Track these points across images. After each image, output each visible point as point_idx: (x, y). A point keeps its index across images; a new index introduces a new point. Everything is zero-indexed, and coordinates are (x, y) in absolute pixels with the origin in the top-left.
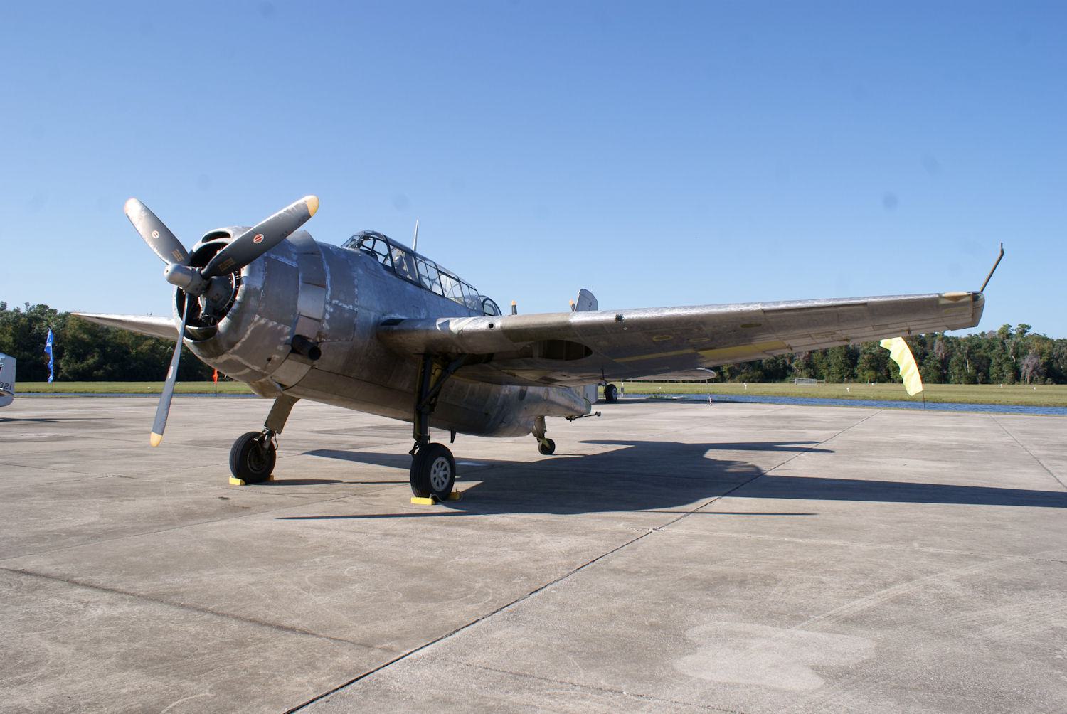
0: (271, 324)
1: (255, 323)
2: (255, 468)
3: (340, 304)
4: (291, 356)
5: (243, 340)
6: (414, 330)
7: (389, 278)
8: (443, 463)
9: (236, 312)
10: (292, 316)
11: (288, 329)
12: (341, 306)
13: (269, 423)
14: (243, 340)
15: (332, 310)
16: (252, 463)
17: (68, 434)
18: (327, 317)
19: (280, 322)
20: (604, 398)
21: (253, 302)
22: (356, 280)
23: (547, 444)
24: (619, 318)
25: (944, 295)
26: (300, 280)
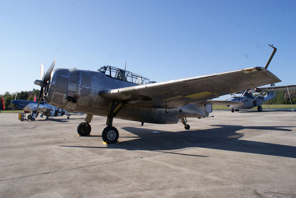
0: (59, 94)
1: (54, 94)
3: (85, 87)
5: (52, 98)
7: (108, 78)
8: (112, 132)
10: (67, 92)
11: (65, 95)
12: (85, 88)
13: (86, 120)
14: (52, 98)
15: (81, 89)
16: (83, 131)
18: (80, 91)
19: (62, 93)
20: (257, 110)
21: (53, 88)
23: (187, 126)
25: (244, 69)
26: (69, 81)
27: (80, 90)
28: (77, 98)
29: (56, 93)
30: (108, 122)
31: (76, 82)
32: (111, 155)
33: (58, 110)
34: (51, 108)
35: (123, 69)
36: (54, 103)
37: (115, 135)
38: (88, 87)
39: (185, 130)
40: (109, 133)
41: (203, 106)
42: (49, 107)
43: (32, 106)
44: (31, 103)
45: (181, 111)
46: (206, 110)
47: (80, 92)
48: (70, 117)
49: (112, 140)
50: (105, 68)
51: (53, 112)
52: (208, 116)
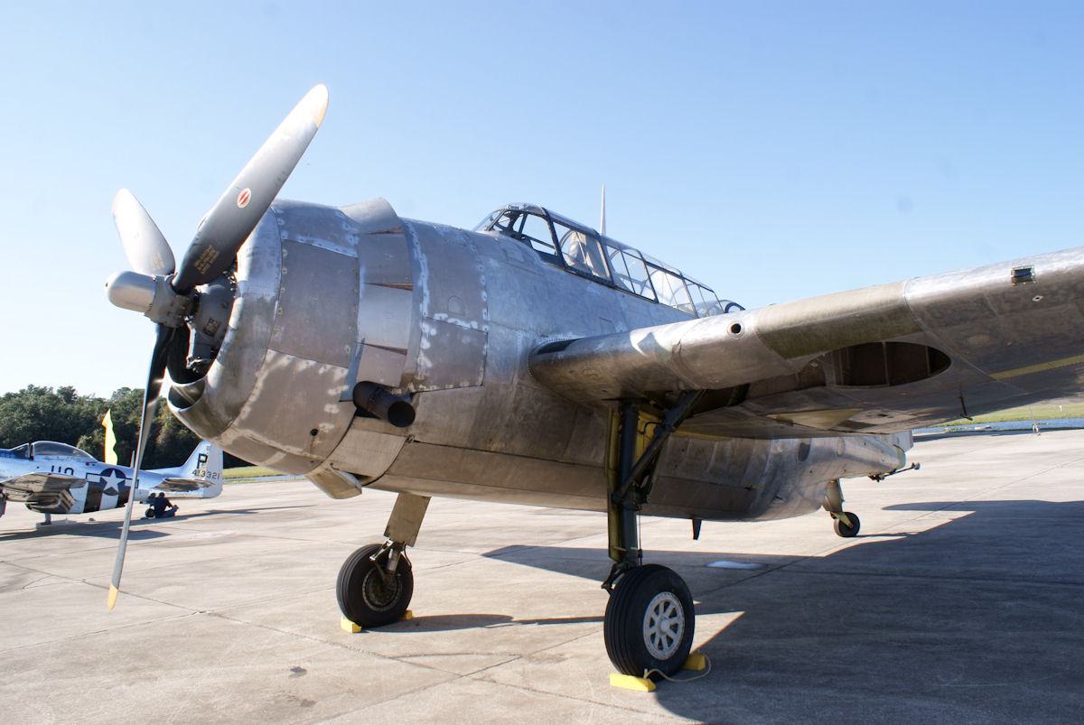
0: (303, 365)
1: (269, 365)
2: (377, 603)
4: (359, 420)
5: (252, 399)
6: (592, 356)
7: (553, 273)
8: (667, 604)
9: (231, 347)
10: (353, 353)
11: (340, 373)
13: (391, 531)
14: (252, 399)
15: (434, 332)
17: (239, 532)
18: (426, 344)
19: (321, 360)
21: (259, 326)
22: (483, 277)
23: (847, 522)
24: (1022, 275)
26: (362, 281)
28: (412, 395)
29: (285, 361)
31: (400, 283)
33: (103, 483)
34: (69, 472)
36: (258, 436)
38: (468, 321)
42: (56, 470)
47: (427, 352)
51: (79, 495)
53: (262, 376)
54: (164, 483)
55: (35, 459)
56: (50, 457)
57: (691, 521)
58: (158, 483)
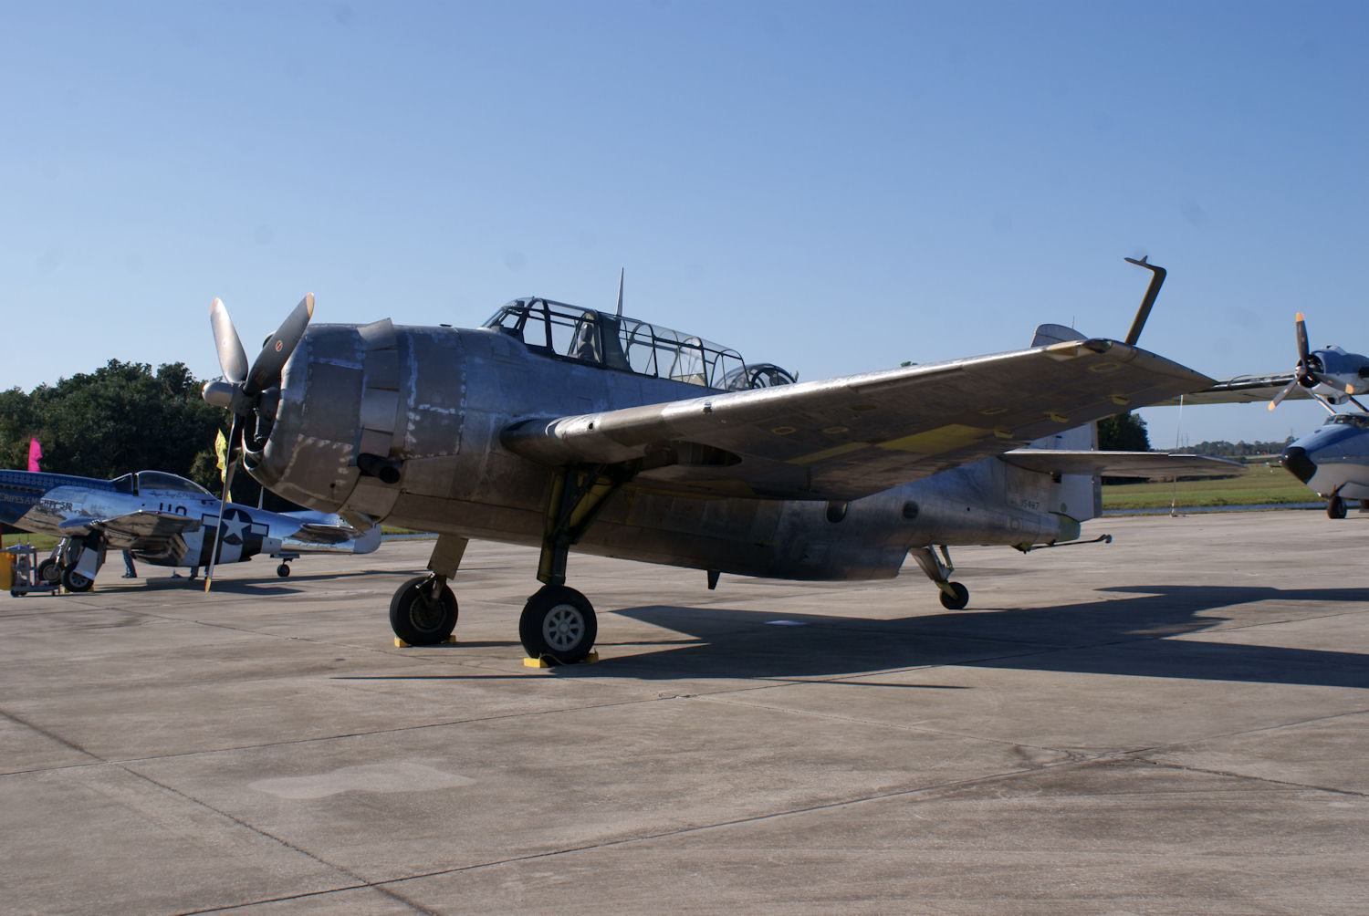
0: (322, 444)
1: (300, 443)
2: (422, 625)
4: (363, 479)
5: (291, 464)
8: (567, 614)
11: (348, 448)
14: (291, 464)
15: (418, 418)
17: (376, 591)
18: (411, 427)
19: (335, 440)
21: (293, 419)
22: (465, 374)
23: (951, 593)
27: (415, 422)
28: (402, 461)
29: (310, 441)
30: (545, 566)
31: (393, 386)
32: (566, 695)
34: (181, 512)
35: (610, 309)
37: (580, 625)
38: (447, 408)
39: (944, 610)
40: (550, 616)
41: (1045, 481)
42: (165, 509)
43: (69, 506)
44: (60, 485)
45: (910, 510)
46: (1064, 507)
47: (412, 433)
48: (296, 567)
49: (565, 647)
50: (522, 311)
51: (193, 541)
52: (1076, 538)
53: (296, 451)
54: (302, 530)
55: (140, 494)
56: (158, 492)
57: (706, 572)
58: (295, 530)
